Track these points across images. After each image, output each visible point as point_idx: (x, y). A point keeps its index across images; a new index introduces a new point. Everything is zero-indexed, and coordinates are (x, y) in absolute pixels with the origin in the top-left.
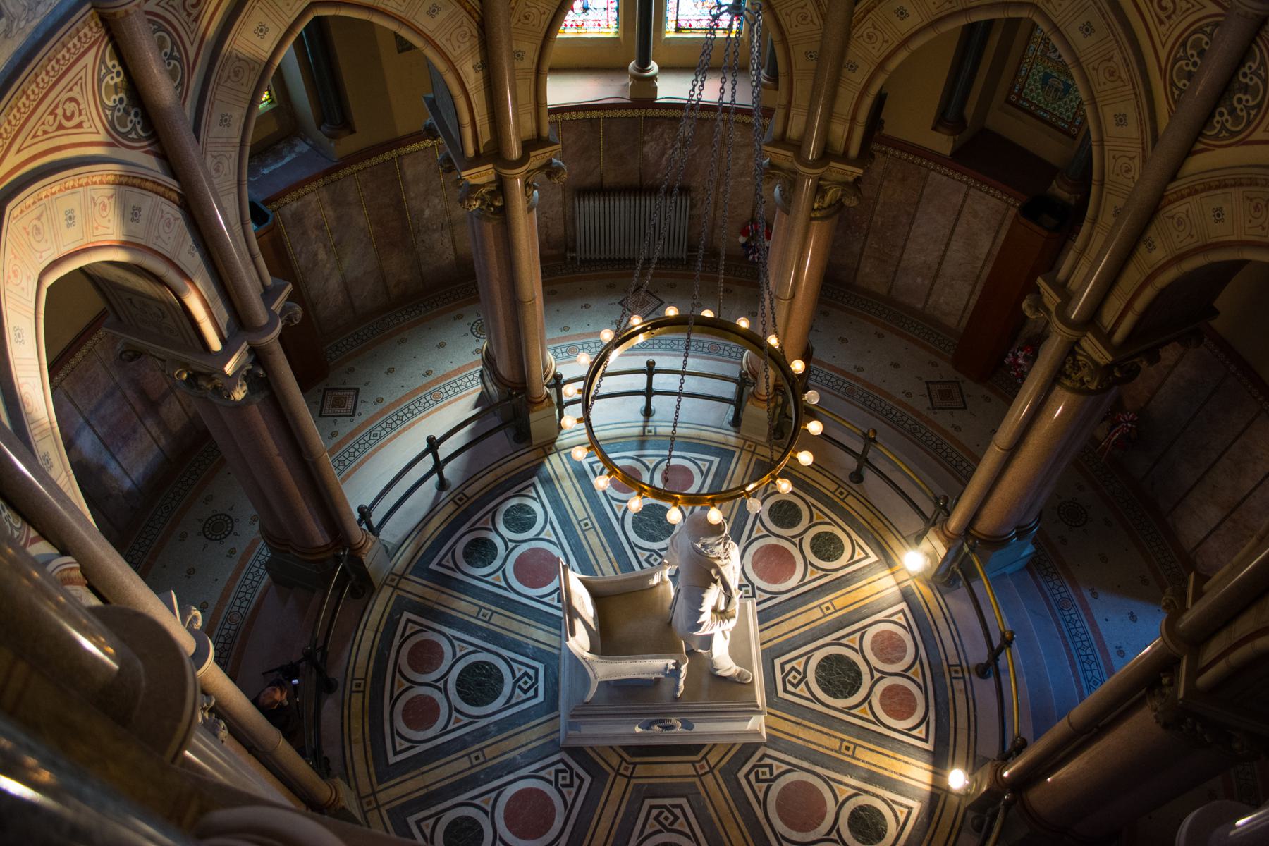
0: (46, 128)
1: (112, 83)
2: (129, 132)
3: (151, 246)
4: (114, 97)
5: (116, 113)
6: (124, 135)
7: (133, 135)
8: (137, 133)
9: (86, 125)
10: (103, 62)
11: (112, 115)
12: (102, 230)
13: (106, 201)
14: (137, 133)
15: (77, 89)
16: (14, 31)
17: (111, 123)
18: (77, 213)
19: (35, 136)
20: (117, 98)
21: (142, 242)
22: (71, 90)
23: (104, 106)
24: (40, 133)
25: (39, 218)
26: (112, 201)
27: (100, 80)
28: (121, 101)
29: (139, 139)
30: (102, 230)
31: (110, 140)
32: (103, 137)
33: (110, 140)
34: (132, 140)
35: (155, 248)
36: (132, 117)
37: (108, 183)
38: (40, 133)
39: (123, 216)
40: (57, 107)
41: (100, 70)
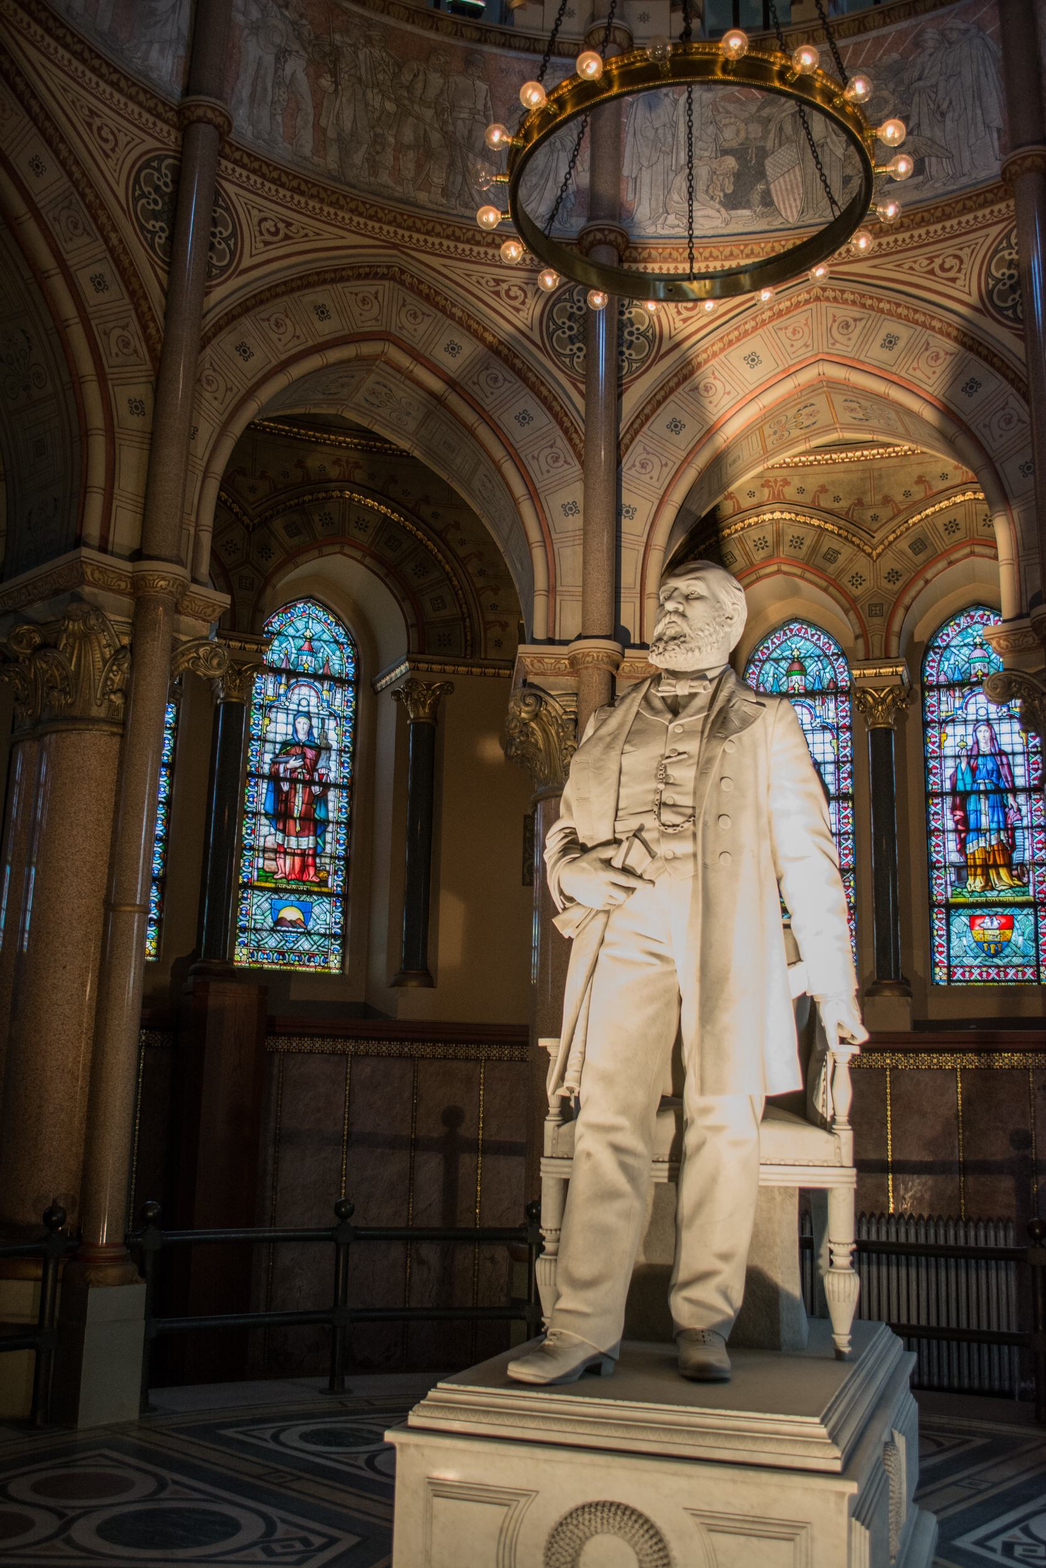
0: (916, 266)
1: (1008, 257)
2: (1007, 309)
3: (973, 428)
4: (1005, 270)
5: (1000, 286)
6: (1000, 310)
7: (1010, 313)
8: (1015, 312)
9: (958, 282)
10: (1008, 237)
11: (994, 286)
12: (918, 373)
13: (942, 354)
14: (1015, 312)
15: (968, 251)
16: (926, 187)
17: (990, 293)
18: (901, 344)
19: (899, 266)
20: (1008, 273)
21: (964, 418)
22: (961, 249)
23: (989, 273)
24: (906, 266)
25: (855, 320)
26: (949, 358)
27: (996, 252)
28: (1011, 277)
29: (1017, 320)
30: (918, 373)
31: (980, 306)
32: (973, 299)
33: (980, 306)
34: (1007, 317)
35: (977, 433)
36: (1017, 296)
37: (948, 335)
38: (906, 266)
39: (955, 379)
40: (938, 256)
41: (1001, 242)
